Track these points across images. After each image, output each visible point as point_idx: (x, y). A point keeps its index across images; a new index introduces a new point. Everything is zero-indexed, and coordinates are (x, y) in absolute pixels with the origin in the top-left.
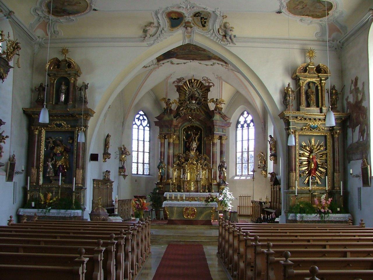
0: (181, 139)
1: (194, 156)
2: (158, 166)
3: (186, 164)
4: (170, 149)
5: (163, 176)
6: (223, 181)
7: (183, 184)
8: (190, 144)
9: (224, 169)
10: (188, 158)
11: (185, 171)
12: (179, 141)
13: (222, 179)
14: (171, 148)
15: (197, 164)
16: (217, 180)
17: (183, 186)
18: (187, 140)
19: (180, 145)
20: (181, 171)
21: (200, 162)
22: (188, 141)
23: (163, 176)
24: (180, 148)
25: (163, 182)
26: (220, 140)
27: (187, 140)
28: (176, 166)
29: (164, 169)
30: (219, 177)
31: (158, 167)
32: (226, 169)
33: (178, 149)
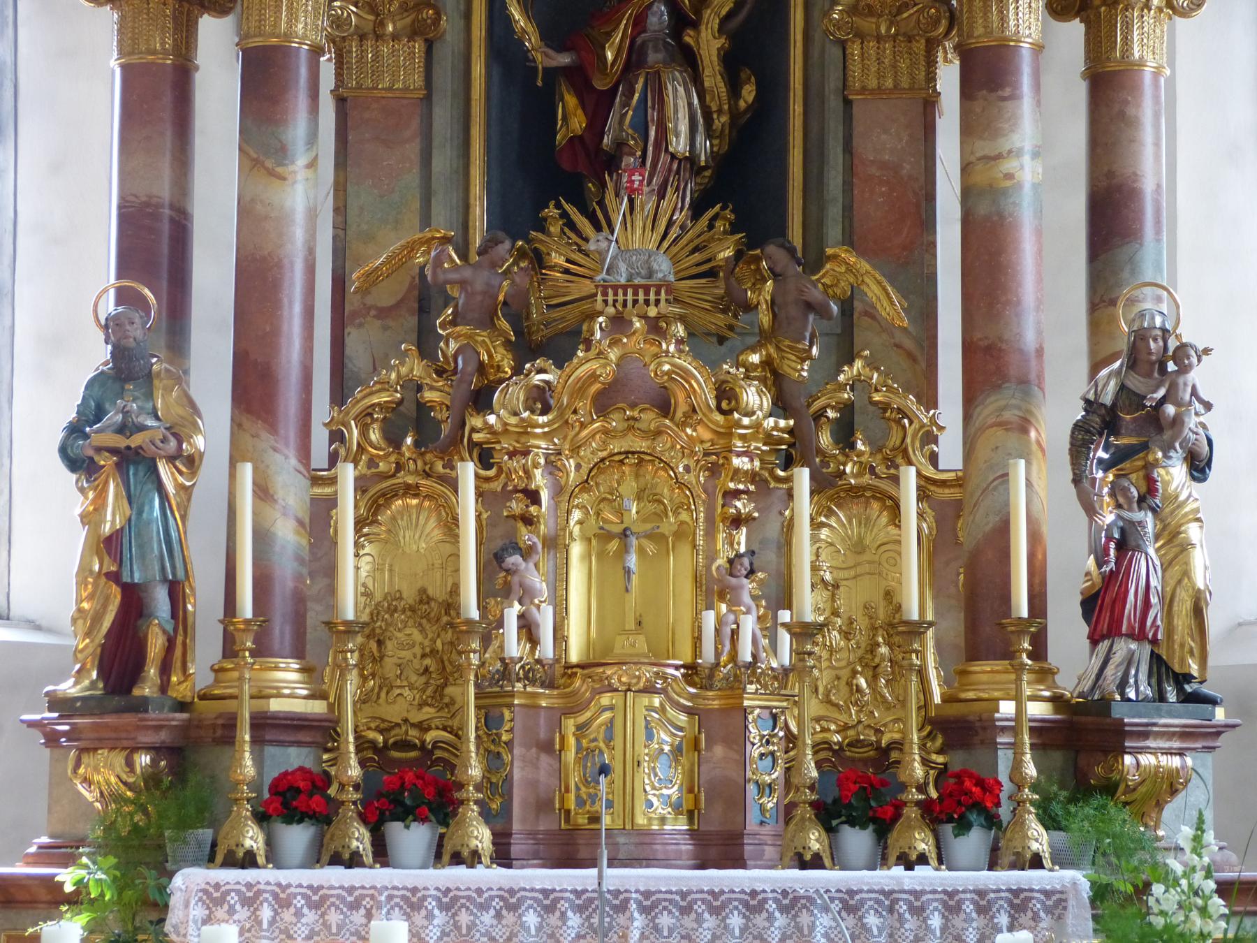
0: (449, 25)
1: (663, 267)
2: (75, 430)
3: (541, 399)
4: (282, 153)
5: (161, 599)
6: (1157, 661)
7: (490, 721)
8: (598, 106)
9: (1175, 474)
10: (571, 313)
11: (516, 506)
12: (418, 47)
13: (1139, 635)
14: (298, 129)
15: (726, 396)
16: (1054, 656)
17: (493, 760)
18: (565, 59)
19: (443, 115)
20: (451, 525)
21: (767, 363)
22: (578, 77)
23: (161, 599)
24: (442, 162)
25: (146, 690)
26: (1075, 29)
27: (565, 59)
28: (375, 436)
29: (164, 470)
30: (1090, 604)
31: (63, 451)
32: (1199, 466)
33: (413, 178)
